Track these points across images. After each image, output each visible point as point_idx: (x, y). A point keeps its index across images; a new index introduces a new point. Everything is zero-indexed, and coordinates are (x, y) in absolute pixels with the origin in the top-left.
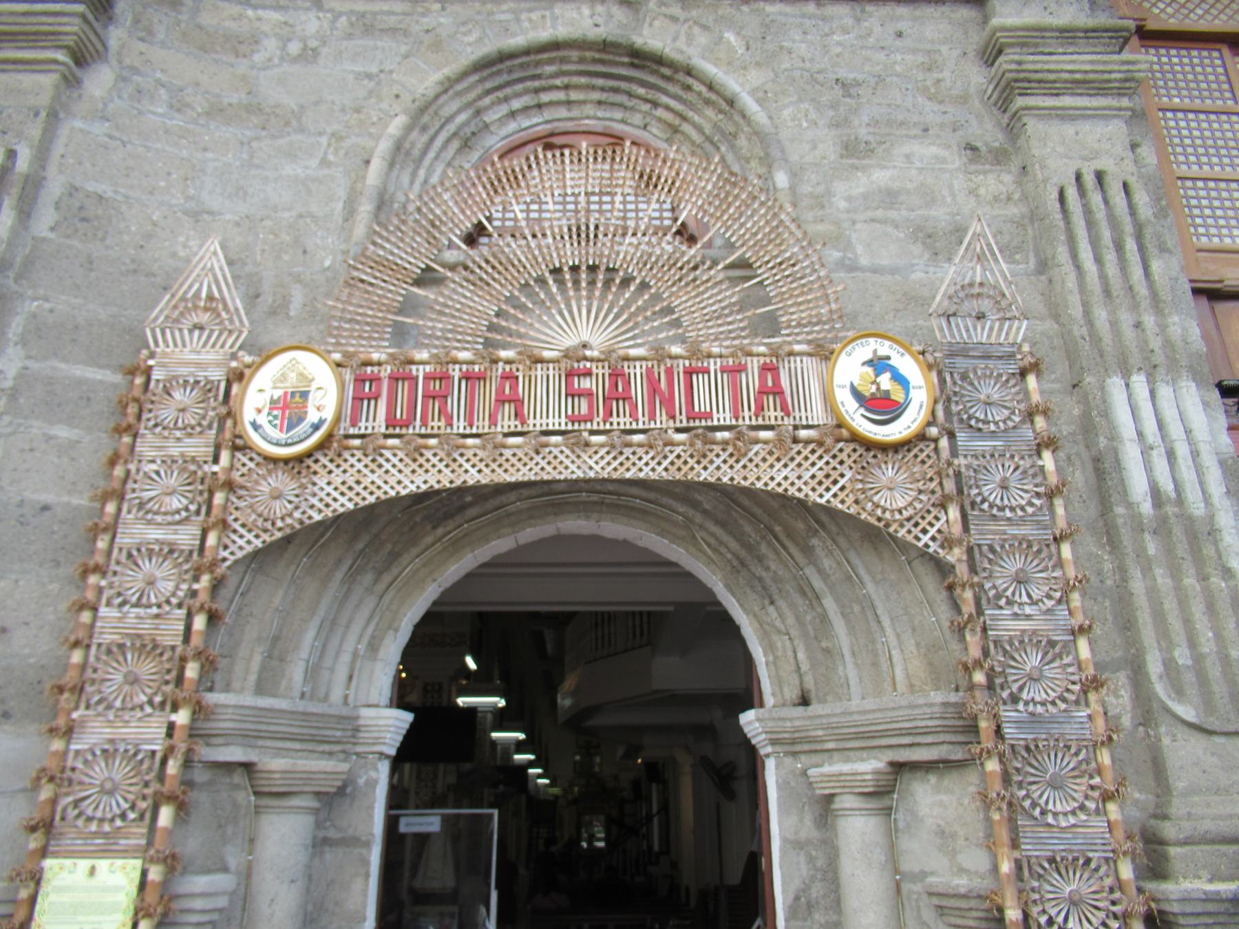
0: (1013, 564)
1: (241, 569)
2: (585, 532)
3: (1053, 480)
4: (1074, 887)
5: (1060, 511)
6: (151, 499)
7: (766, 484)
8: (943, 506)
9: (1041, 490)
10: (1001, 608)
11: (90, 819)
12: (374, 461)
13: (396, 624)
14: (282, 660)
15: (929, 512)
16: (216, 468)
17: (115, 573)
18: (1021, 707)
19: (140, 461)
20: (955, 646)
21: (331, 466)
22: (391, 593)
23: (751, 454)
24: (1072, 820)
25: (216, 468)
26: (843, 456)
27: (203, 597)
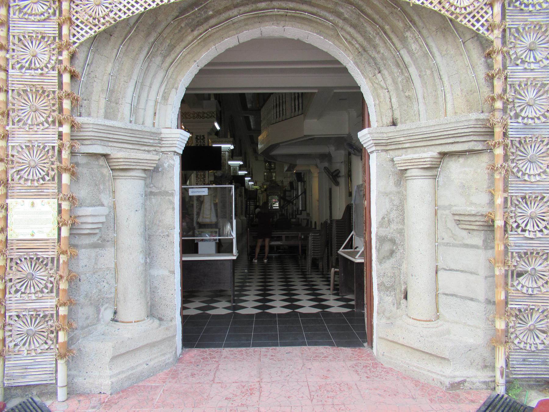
0: (528, 40)
4: (533, 210)
6: (25, 7)
10: (517, 65)
11: (27, 180)
13: (176, 85)
14: (117, 104)
15: (482, 9)
17: (13, 50)
18: (520, 120)
24: (538, 178)
27: (66, 63)
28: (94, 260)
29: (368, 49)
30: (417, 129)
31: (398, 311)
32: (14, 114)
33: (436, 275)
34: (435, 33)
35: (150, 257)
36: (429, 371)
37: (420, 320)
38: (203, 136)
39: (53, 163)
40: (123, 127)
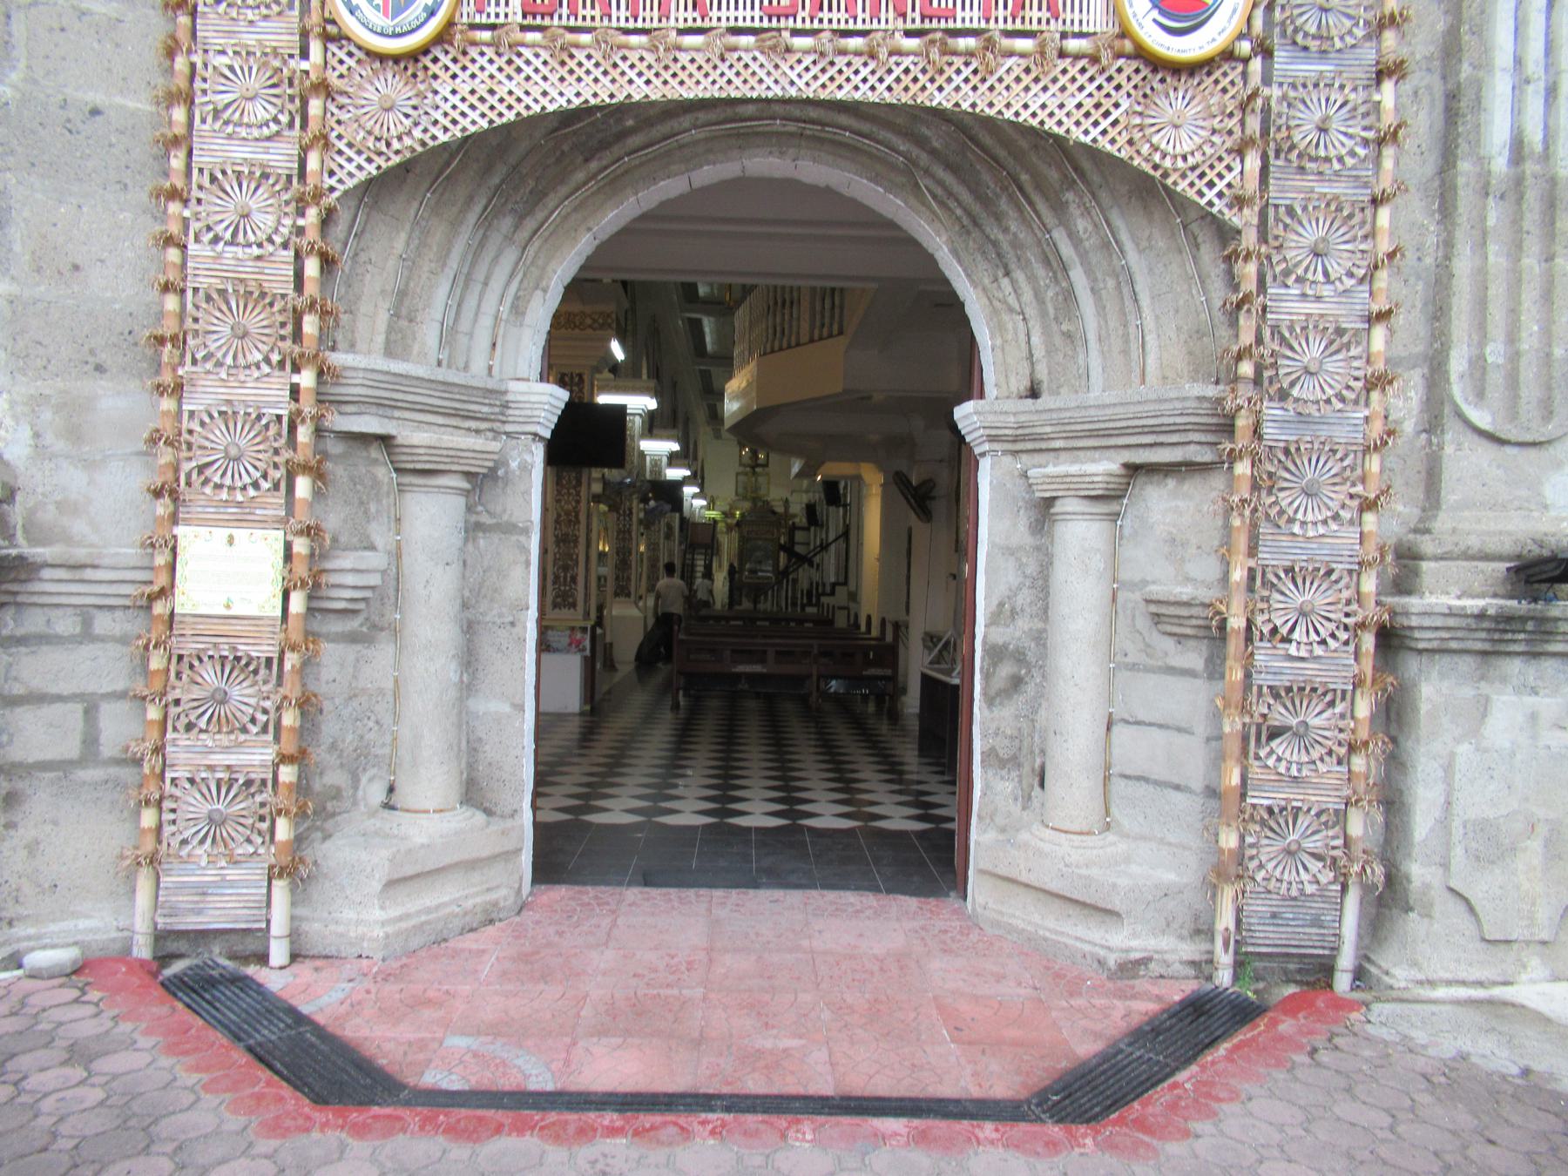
0: (1311, 234)
1: (353, 203)
2: (777, 174)
3: (1388, 119)
4: (1308, 597)
5: (1388, 163)
6: (228, 106)
7: (1017, 114)
8: (1240, 152)
9: (1370, 135)
10: (1287, 286)
11: (218, 487)
12: (510, 62)
13: (544, 283)
14: (411, 321)
16: (305, 65)
17: (199, 201)
18: (1290, 405)
19: (206, 51)
20: (1224, 332)
21: (455, 68)
22: (536, 243)
23: (1001, 72)
24: (1321, 530)
25: (305, 65)
26: (1121, 79)
27: (312, 235)
32: (198, 341)
36: (1077, 938)
38: (580, 376)
39: (276, 452)
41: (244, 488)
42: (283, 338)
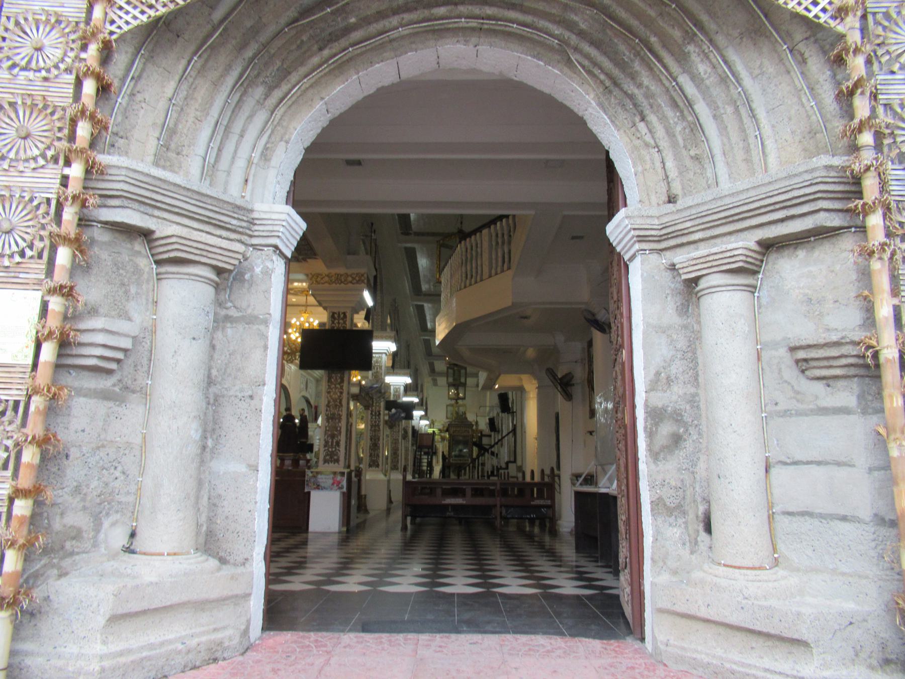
1: (131, 50)
10: (893, 73)
13: (287, 137)
14: (178, 154)
28: (102, 424)
29: (622, 81)
30: (714, 202)
31: (693, 557)
33: (766, 477)
34: (738, 40)
35: (215, 437)
37: (739, 568)
38: (344, 314)
40: (183, 185)
41: (11, 256)
42: (59, 139)
